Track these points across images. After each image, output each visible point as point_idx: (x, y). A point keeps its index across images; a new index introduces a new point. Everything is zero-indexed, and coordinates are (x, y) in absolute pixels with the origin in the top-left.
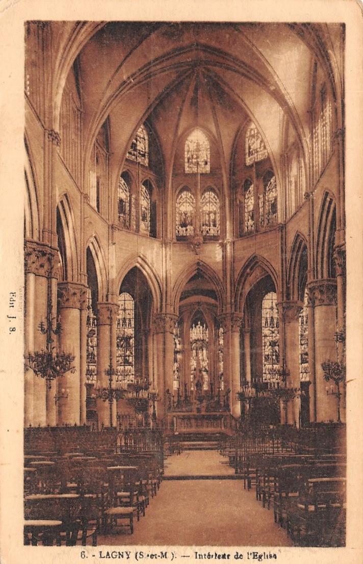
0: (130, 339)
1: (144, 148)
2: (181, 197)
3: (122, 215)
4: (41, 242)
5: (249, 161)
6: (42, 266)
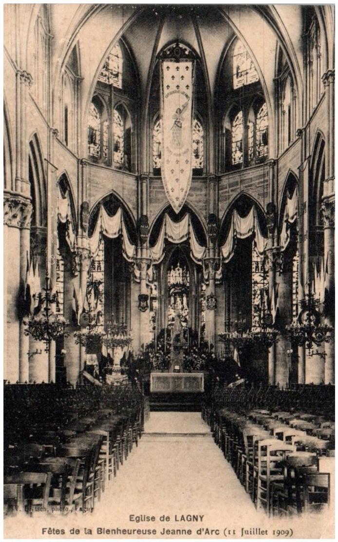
0: (99, 285)
1: (117, 67)
3: (92, 145)
4: (14, 192)
5: (237, 84)
6: (14, 216)
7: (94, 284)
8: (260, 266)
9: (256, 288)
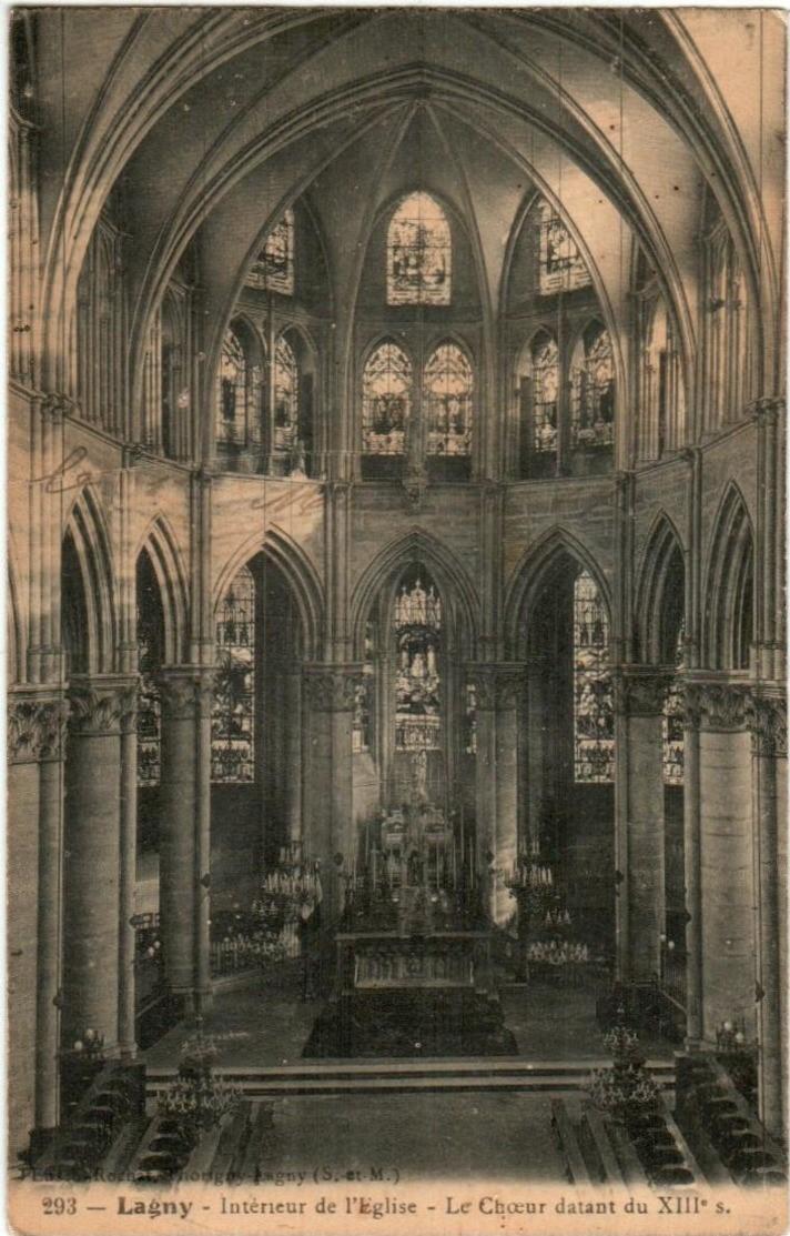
0: (244, 675)
1: (282, 248)
2: (377, 358)
5: (547, 283)
7: (232, 674)
8: (590, 632)
9: (582, 680)
